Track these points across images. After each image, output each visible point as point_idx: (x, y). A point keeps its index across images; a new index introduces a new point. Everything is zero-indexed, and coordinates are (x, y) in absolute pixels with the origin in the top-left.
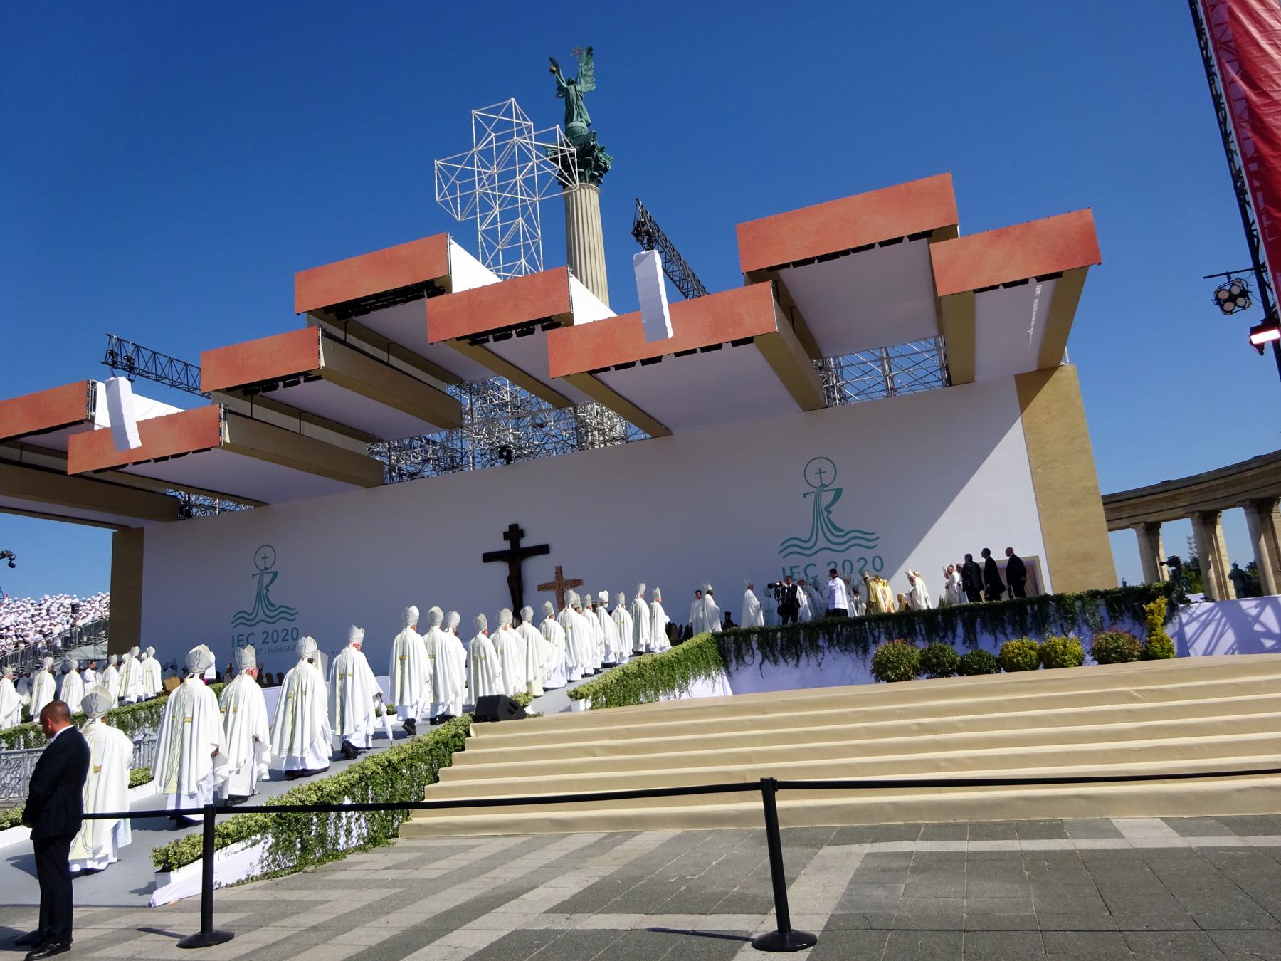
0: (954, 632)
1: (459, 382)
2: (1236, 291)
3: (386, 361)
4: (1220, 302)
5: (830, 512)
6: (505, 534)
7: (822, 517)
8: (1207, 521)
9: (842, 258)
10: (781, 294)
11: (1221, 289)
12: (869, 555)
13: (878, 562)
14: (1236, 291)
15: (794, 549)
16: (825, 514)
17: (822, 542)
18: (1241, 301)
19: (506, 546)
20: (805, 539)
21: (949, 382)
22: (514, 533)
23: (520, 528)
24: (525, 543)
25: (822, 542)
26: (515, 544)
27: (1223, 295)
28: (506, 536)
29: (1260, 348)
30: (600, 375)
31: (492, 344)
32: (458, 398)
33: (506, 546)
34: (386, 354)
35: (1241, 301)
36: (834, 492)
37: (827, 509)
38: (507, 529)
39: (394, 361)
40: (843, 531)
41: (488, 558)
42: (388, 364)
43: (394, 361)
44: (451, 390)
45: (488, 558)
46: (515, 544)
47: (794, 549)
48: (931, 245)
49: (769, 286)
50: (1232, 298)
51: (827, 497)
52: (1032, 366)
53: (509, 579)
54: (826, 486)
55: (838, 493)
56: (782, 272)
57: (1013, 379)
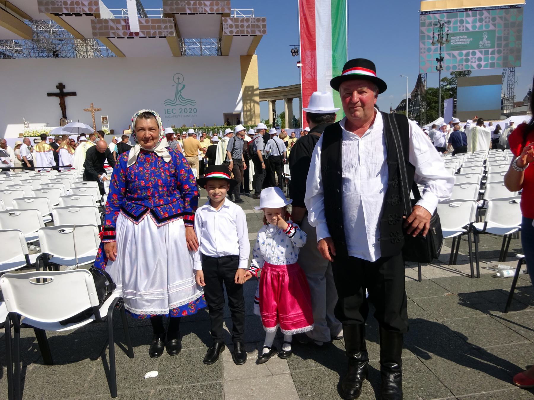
0: (220, 133)
1: (31, 20)
2: (296, 51)
3: (5, 9)
4: (292, 52)
5: (181, 92)
6: (57, 86)
7: (178, 93)
8: (289, 101)
9: (196, 15)
10: (176, 24)
11: (293, 49)
12: (193, 107)
13: (195, 109)
14: (296, 51)
15: (168, 103)
16: (179, 93)
17: (178, 102)
18: (296, 54)
19: (58, 91)
20: (173, 100)
21: (221, 55)
22: (61, 86)
23: (64, 85)
24: (65, 91)
25: (178, 102)
26: (61, 90)
27: (293, 51)
28: (57, 87)
29: (299, 67)
30: (110, 39)
31: (63, 17)
32: (30, 26)
33: (58, 91)
34: (5, 7)
35: (296, 54)
36: (182, 86)
37: (180, 91)
38: (58, 85)
39: (8, 10)
40: (184, 99)
41: (50, 95)
42: (6, 11)
43: (8, 10)
44: (27, 22)
45: (50, 95)
46: (61, 90)
47: (168, 103)
48: (223, 18)
49: (172, 19)
50: (295, 52)
51: (180, 87)
52: (245, 53)
53: (60, 104)
54: (180, 83)
55: (184, 86)
56: (175, 15)
57: (240, 57)
